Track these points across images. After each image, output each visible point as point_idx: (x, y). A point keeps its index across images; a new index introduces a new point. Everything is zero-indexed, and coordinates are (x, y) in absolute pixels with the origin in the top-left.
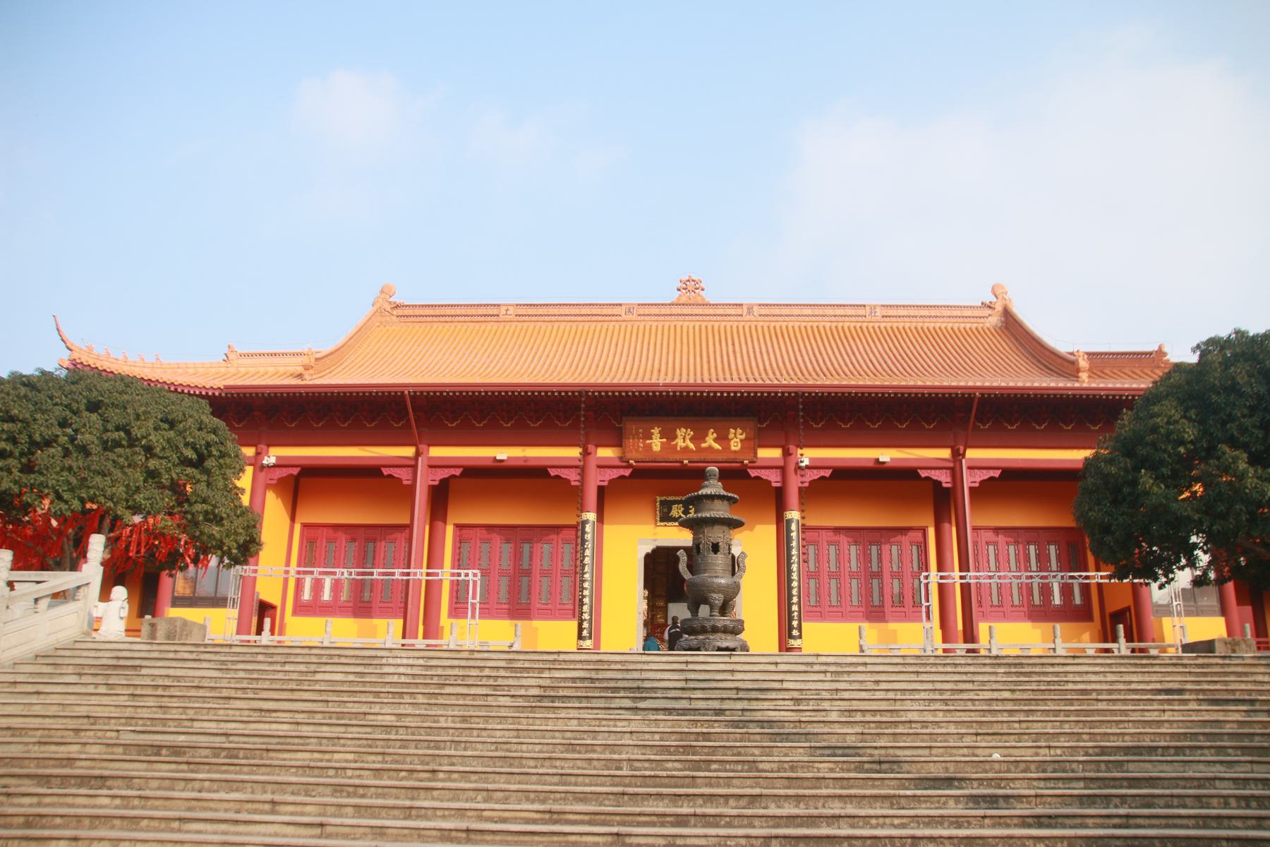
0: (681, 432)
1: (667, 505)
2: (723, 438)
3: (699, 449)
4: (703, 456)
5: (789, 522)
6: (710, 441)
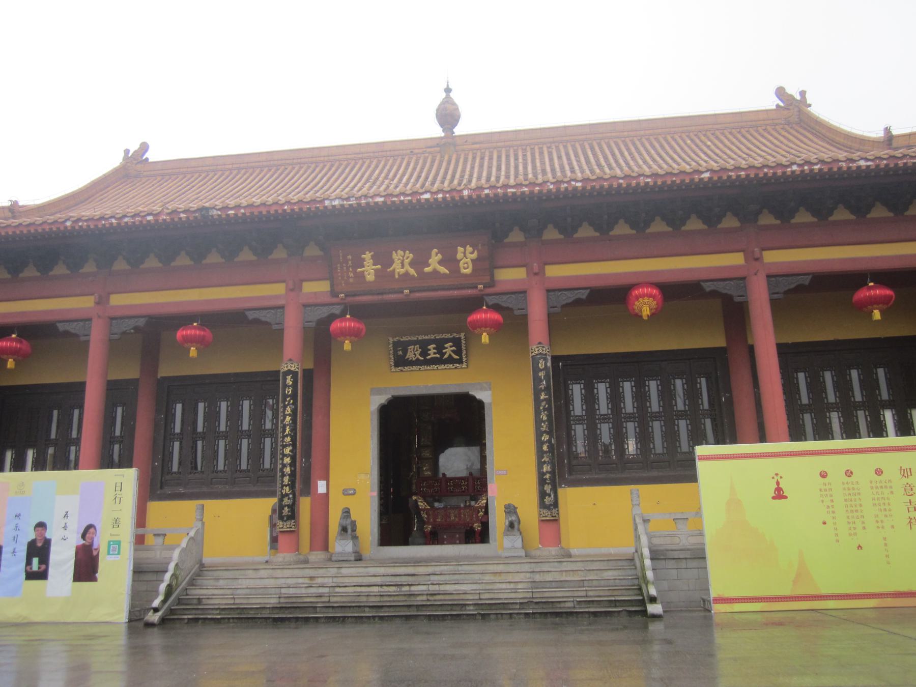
0: (397, 256)
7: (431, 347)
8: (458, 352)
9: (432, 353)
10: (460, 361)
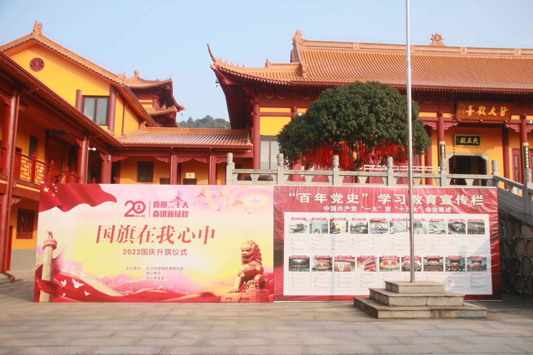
0: (481, 108)
1: (459, 138)
2: (498, 111)
3: (487, 115)
4: (488, 118)
5: (525, 147)
6: (493, 112)
7: (469, 139)
8: (479, 141)
9: (469, 141)
10: (479, 145)
